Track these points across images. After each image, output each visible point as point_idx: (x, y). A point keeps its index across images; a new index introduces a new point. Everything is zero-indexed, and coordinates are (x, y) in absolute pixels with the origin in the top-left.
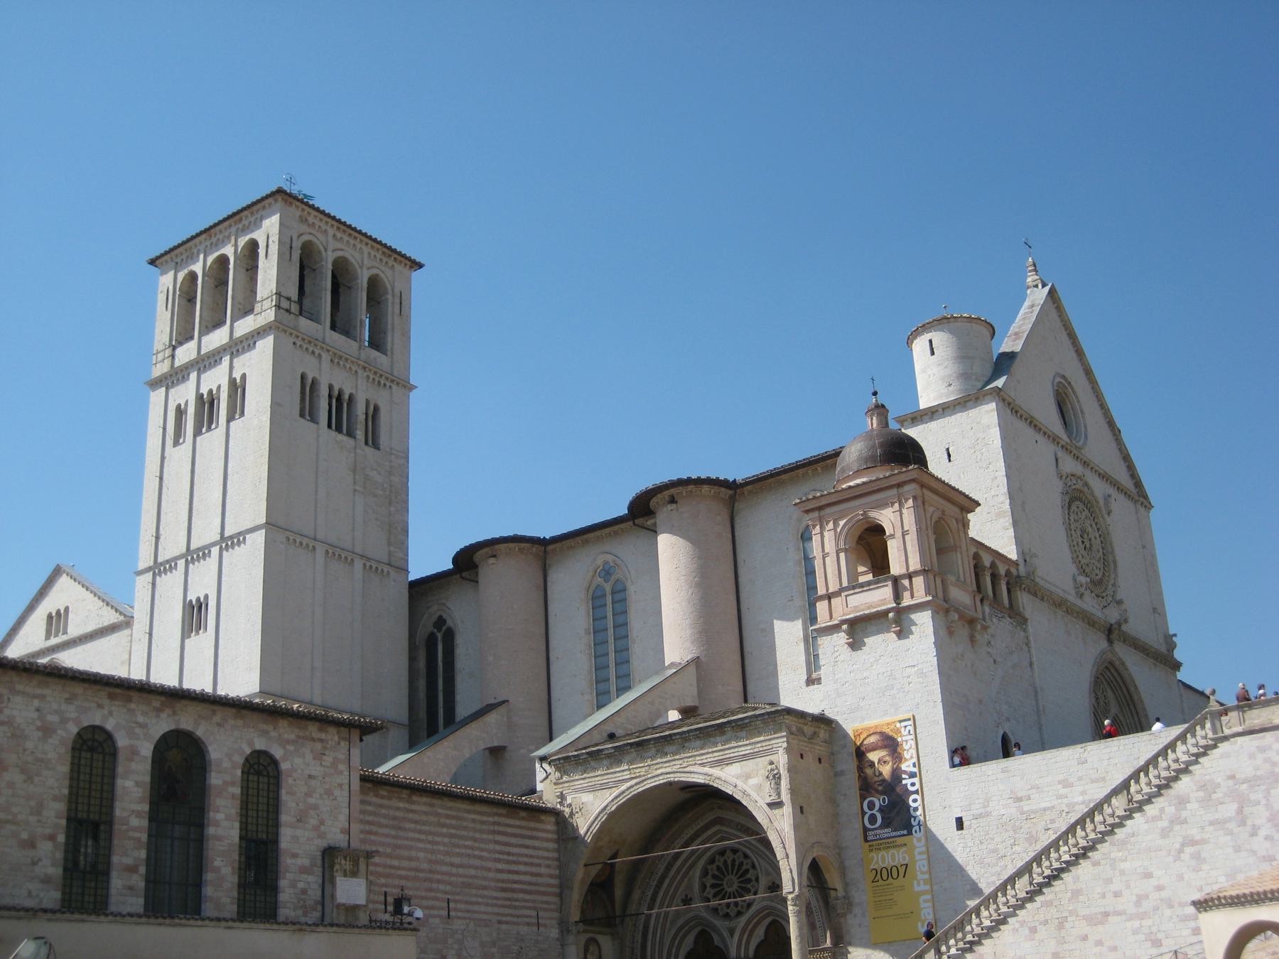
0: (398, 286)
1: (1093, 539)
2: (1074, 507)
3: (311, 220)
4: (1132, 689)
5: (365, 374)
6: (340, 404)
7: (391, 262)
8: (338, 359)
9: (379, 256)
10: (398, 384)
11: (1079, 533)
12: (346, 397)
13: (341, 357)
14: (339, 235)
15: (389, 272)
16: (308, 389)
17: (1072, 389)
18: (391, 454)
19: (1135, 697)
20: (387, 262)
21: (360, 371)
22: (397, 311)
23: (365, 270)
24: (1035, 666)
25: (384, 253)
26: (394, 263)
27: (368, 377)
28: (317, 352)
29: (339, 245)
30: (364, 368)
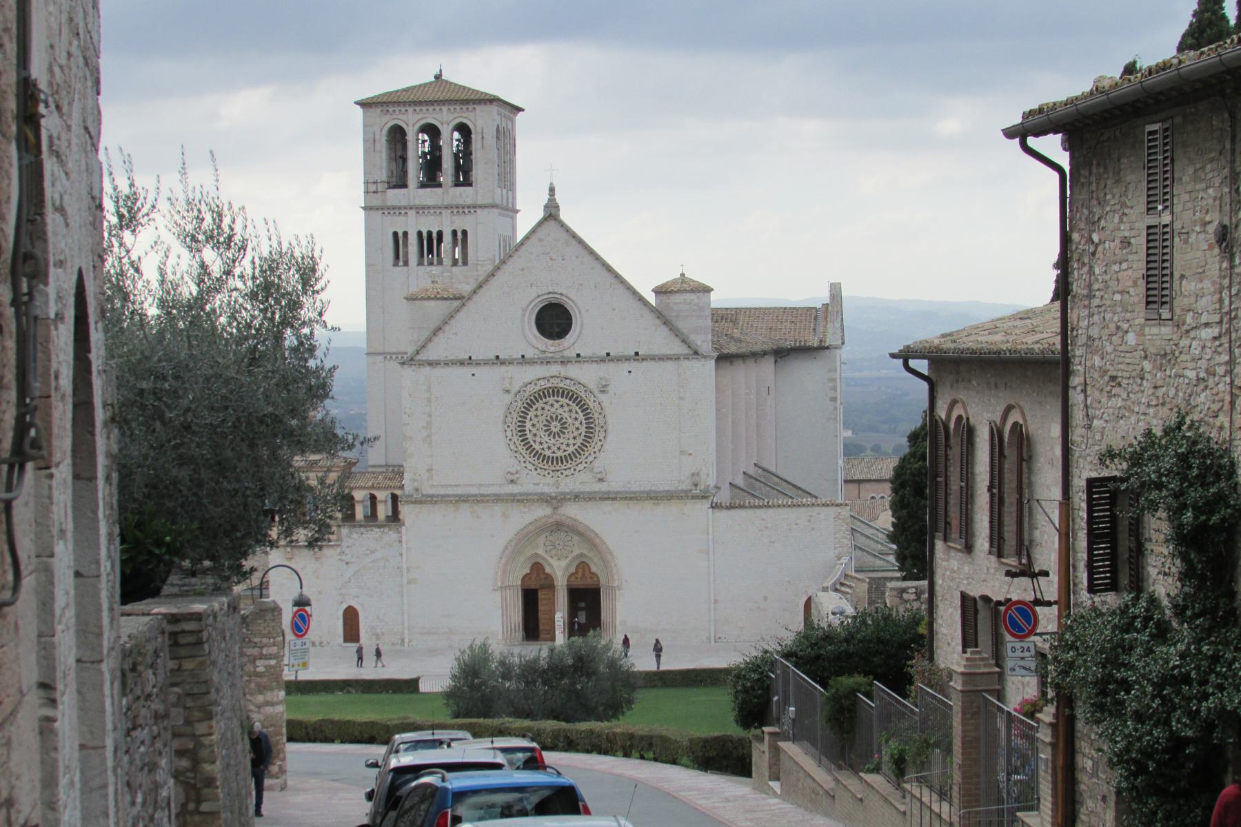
0: (480, 124)
1: (570, 421)
2: (540, 405)
3: (391, 110)
4: (593, 535)
6: (430, 244)
7: (471, 107)
8: (421, 209)
9: (458, 108)
10: (480, 206)
11: (540, 426)
12: (435, 235)
13: (423, 208)
14: (418, 109)
15: (471, 115)
16: (398, 240)
17: (569, 299)
18: (477, 265)
19: (597, 541)
21: (444, 212)
22: (479, 145)
23: (445, 126)
24: (404, 556)
25: (461, 104)
29: (421, 116)
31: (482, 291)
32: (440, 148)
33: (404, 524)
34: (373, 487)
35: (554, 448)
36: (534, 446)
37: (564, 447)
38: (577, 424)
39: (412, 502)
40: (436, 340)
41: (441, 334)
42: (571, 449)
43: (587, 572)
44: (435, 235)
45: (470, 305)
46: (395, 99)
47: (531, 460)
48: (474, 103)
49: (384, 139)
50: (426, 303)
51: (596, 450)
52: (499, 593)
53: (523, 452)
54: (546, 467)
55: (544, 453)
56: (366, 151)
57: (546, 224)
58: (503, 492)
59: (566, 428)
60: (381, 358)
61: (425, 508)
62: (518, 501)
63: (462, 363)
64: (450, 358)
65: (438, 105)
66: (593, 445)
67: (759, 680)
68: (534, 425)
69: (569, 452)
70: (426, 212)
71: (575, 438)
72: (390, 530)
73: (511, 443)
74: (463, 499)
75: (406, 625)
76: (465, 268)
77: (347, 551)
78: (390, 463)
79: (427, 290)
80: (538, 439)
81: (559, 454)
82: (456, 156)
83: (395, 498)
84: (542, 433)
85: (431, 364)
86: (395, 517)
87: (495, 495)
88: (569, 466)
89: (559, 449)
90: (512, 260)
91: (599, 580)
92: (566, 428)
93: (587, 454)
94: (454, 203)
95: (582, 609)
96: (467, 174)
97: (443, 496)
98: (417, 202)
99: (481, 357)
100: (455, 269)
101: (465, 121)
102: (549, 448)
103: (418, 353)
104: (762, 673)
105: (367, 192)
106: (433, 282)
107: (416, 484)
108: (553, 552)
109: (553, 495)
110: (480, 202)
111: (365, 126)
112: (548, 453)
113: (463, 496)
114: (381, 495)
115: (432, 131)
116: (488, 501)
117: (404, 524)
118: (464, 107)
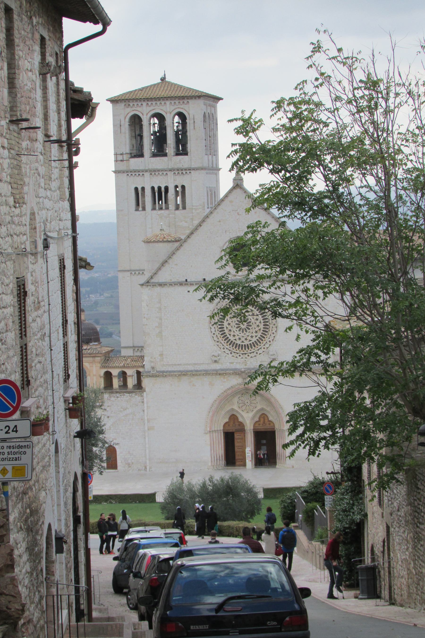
5: (173, 173)
7: (185, 101)
8: (153, 172)
10: (194, 169)
12: (163, 189)
14: (150, 103)
15: (186, 107)
18: (192, 209)
19: (273, 400)
20: (183, 102)
21: (169, 173)
22: (192, 127)
23: (168, 114)
25: (179, 99)
26: (189, 101)
27: (175, 173)
28: (141, 174)
29: (152, 108)
30: (170, 170)
31: (193, 236)
32: (165, 128)
33: (145, 391)
34: (124, 367)
35: (243, 339)
36: (230, 338)
37: (249, 338)
38: (258, 323)
39: (150, 376)
40: (164, 269)
41: (167, 265)
42: (254, 339)
43: (266, 421)
44: (163, 189)
45: (185, 245)
46: (134, 97)
47: (228, 347)
48: (188, 99)
49: (127, 124)
50: (156, 245)
51: (270, 340)
52: (208, 435)
53: (223, 342)
54: (238, 352)
55: (236, 342)
56: (115, 133)
57: (235, 191)
58: (210, 368)
59: (250, 326)
60: (128, 273)
61: (159, 380)
62: (220, 374)
63: (181, 284)
64: (173, 280)
65: (163, 100)
66: (268, 336)
67: (291, 503)
68: (229, 324)
69: (253, 341)
70: (157, 173)
71: (256, 332)
72: (136, 395)
73: (215, 336)
74: (183, 374)
75: (148, 457)
76: (184, 211)
77: (108, 409)
78: (135, 345)
79: (157, 236)
80: (232, 333)
81: (246, 343)
82: (177, 134)
83: (139, 373)
84: (235, 329)
85: (161, 285)
86: (139, 386)
87: (204, 371)
88: (253, 351)
89: (246, 339)
90: (213, 215)
91: (274, 426)
92: (250, 326)
93: (264, 342)
94: (176, 167)
95: (264, 445)
96: (185, 146)
97: (170, 372)
98: (150, 167)
99: (193, 280)
100: (177, 212)
101: (182, 111)
102: (240, 339)
103: (152, 278)
104: (292, 500)
105: (116, 161)
106: (161, 230)
107: (152, 365)
108: (244, 408)
109: (243, 370)
110: (193, 167)
111: (114, 116)
112: (239, 342)
113: (184, 371)
114: (130, 372)
115: (161, 117)
116: (200, 375)
117: (145, 391)
118: (181, 102)
